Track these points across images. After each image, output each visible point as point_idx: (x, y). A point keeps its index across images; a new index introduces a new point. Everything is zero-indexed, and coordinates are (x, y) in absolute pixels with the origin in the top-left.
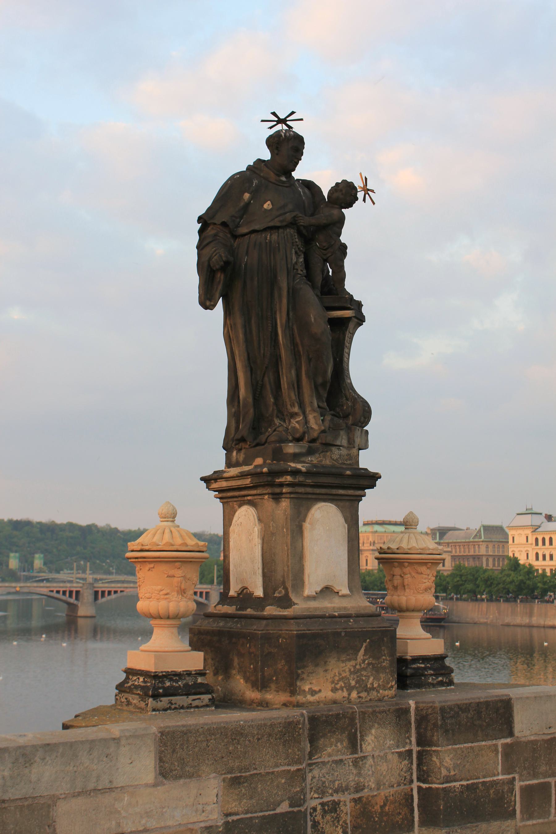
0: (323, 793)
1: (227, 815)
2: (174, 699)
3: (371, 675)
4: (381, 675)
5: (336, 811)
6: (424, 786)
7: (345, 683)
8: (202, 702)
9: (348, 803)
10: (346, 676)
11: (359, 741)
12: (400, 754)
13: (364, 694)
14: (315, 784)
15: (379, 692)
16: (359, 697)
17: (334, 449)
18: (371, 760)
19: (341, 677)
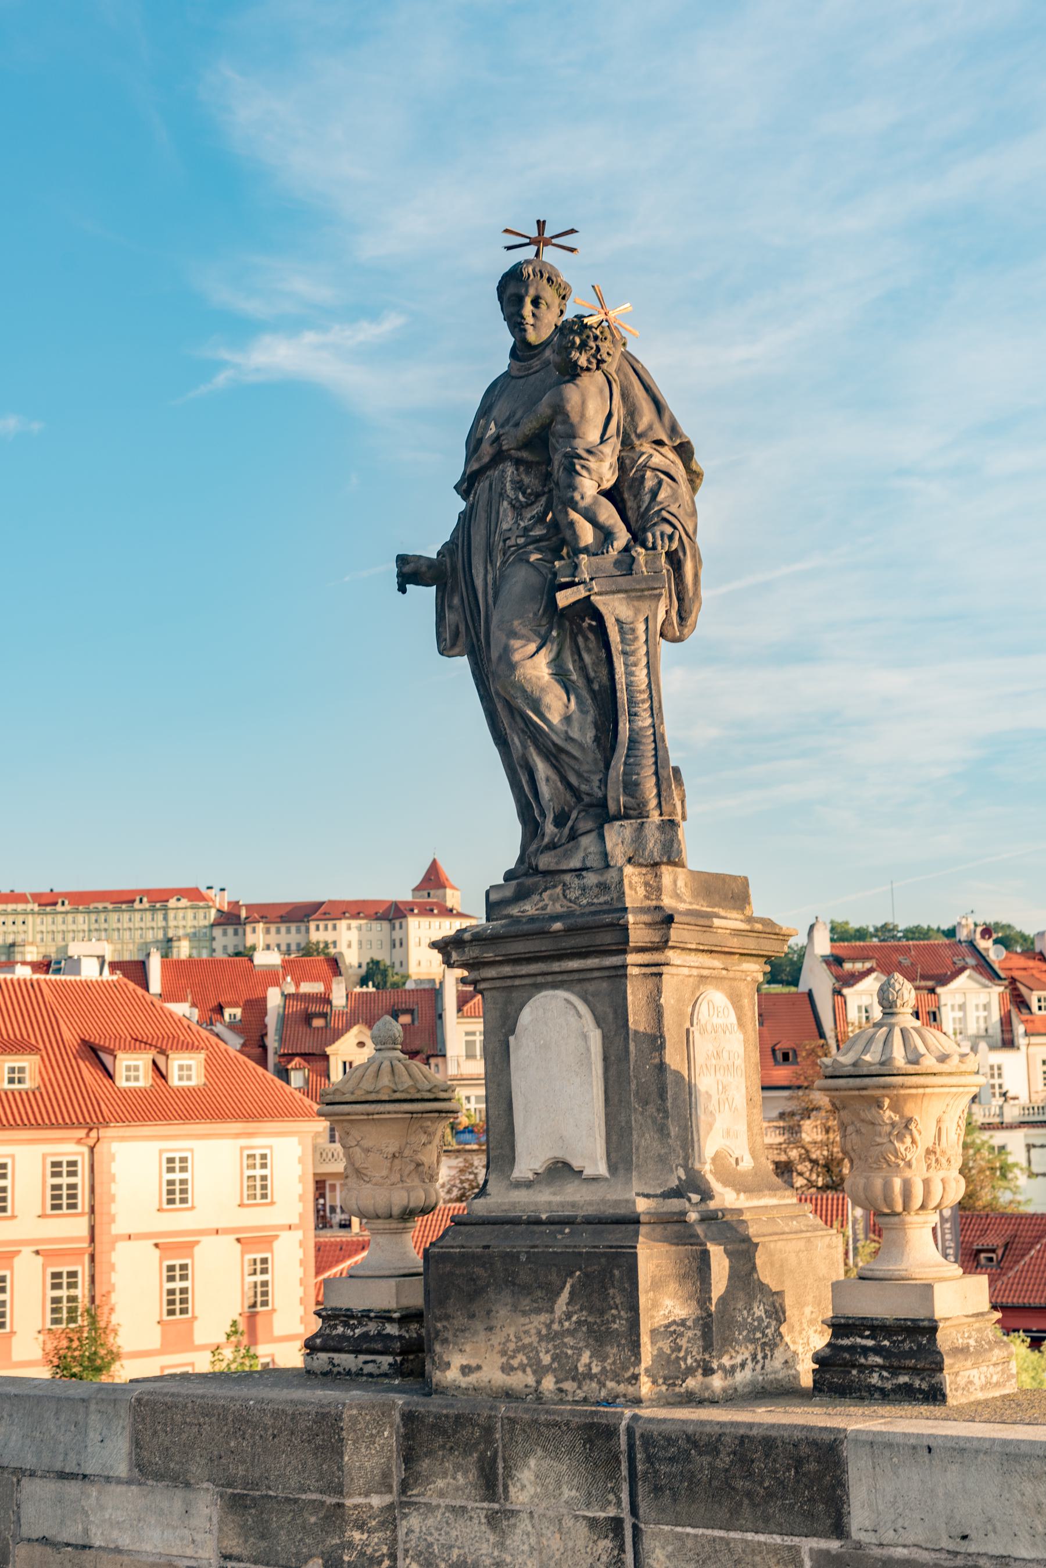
3: (586, 1347)
4: (608, 1348)
7: (528, 1358)
10: (531, 1344)
11: (500, 1478)
13: (569, 1386)
15: (604, 1385)
16: (561, 1390)
17: (567, 878)
18: (527, 1522)
19: (520, 1344)
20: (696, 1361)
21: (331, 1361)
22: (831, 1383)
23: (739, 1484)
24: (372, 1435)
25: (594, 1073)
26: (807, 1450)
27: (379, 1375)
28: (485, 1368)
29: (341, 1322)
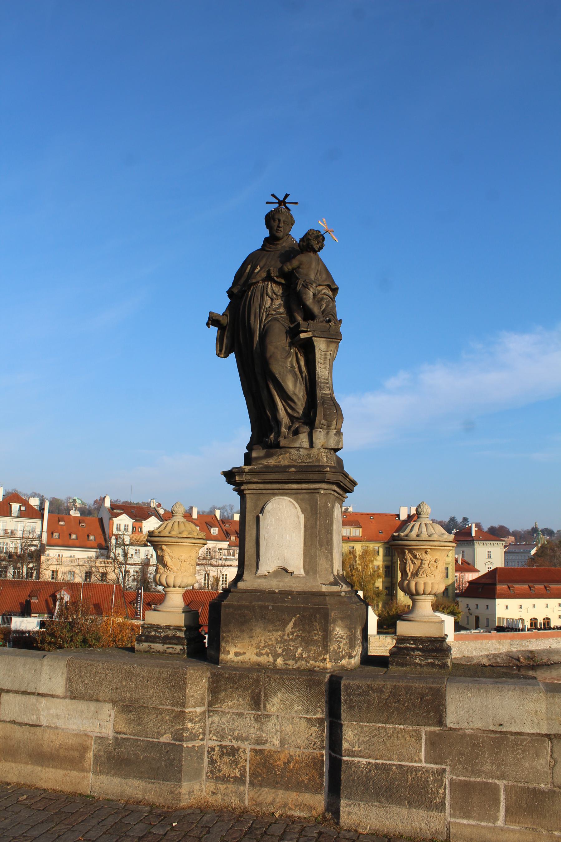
0: (222, 737)
1: (117, 733)
2: (153, 645)
4: (312, 647)
5: (234, 756)
6: (333, 754)
7: (271, 650)
8: (175, 650)
9: (248, 751)
10: (272, 644)
12: (309, 721)
13: (291, 662)
14: (214, 728)
15: (309, 662)
16: (286, 664)
17: (292, 451)
18: (275, 719)
19: (266, 644)
23: (393, 705)
24: (198, 682)
26: (427, 691)
27: (174, 654)
28: (247, 654)
29: (154, 630)
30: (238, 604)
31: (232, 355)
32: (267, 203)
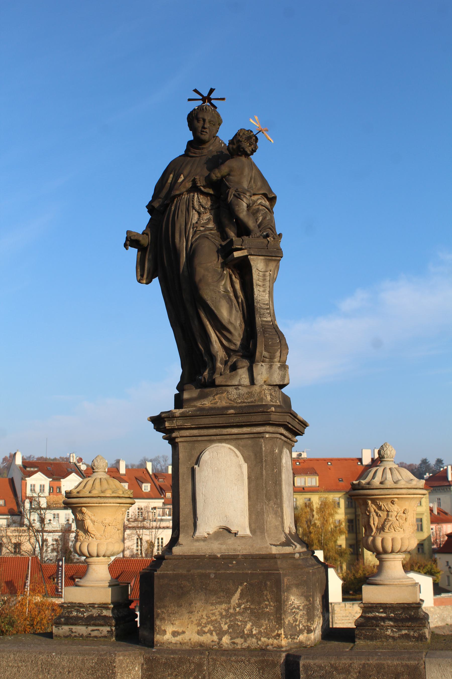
2: (74, 628)
3: (249, 621)
4: (263, 621)
7: (214, 627)
10: (216, 620)
13: (239, 641)
15: (260, 640)
16: (234, 643)
17: (230, 389)
19: (209, 620)
20: (304, 626)
21: (71, 630)
22: (365, 635)
24: (129, 670)
25: (245, 484)
27: (100, 637)
28: (187, 633)
29: (75, 609)
30: (173, 573)
31: (156, 281)
32: (189, 100)
